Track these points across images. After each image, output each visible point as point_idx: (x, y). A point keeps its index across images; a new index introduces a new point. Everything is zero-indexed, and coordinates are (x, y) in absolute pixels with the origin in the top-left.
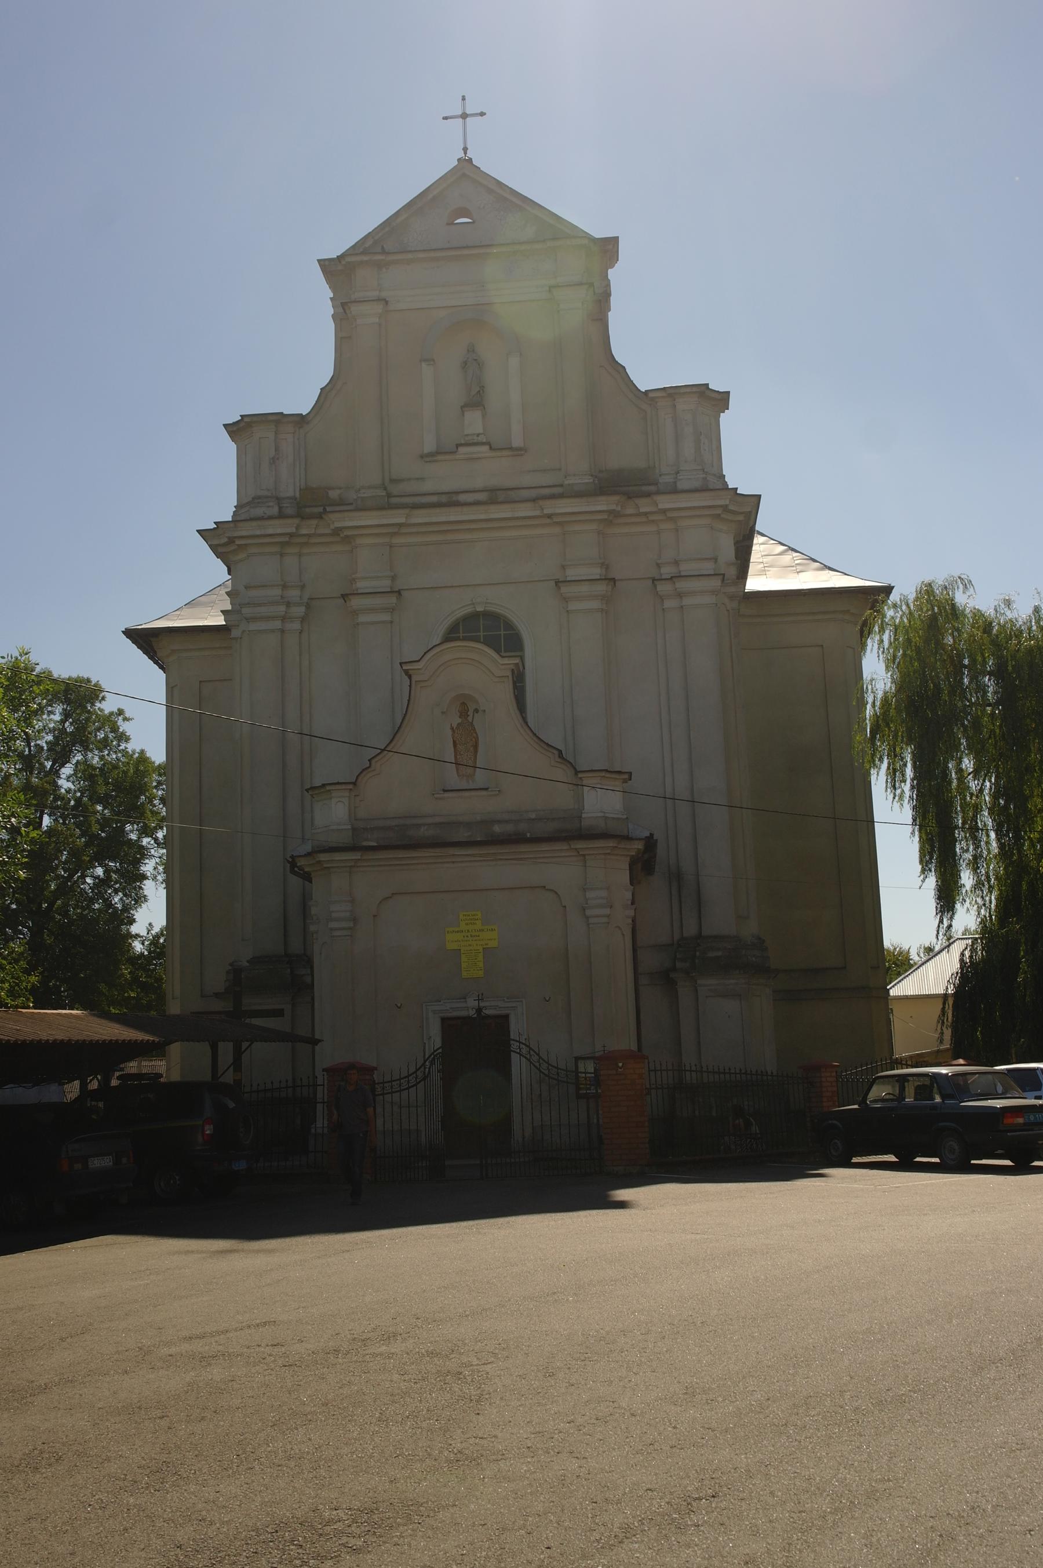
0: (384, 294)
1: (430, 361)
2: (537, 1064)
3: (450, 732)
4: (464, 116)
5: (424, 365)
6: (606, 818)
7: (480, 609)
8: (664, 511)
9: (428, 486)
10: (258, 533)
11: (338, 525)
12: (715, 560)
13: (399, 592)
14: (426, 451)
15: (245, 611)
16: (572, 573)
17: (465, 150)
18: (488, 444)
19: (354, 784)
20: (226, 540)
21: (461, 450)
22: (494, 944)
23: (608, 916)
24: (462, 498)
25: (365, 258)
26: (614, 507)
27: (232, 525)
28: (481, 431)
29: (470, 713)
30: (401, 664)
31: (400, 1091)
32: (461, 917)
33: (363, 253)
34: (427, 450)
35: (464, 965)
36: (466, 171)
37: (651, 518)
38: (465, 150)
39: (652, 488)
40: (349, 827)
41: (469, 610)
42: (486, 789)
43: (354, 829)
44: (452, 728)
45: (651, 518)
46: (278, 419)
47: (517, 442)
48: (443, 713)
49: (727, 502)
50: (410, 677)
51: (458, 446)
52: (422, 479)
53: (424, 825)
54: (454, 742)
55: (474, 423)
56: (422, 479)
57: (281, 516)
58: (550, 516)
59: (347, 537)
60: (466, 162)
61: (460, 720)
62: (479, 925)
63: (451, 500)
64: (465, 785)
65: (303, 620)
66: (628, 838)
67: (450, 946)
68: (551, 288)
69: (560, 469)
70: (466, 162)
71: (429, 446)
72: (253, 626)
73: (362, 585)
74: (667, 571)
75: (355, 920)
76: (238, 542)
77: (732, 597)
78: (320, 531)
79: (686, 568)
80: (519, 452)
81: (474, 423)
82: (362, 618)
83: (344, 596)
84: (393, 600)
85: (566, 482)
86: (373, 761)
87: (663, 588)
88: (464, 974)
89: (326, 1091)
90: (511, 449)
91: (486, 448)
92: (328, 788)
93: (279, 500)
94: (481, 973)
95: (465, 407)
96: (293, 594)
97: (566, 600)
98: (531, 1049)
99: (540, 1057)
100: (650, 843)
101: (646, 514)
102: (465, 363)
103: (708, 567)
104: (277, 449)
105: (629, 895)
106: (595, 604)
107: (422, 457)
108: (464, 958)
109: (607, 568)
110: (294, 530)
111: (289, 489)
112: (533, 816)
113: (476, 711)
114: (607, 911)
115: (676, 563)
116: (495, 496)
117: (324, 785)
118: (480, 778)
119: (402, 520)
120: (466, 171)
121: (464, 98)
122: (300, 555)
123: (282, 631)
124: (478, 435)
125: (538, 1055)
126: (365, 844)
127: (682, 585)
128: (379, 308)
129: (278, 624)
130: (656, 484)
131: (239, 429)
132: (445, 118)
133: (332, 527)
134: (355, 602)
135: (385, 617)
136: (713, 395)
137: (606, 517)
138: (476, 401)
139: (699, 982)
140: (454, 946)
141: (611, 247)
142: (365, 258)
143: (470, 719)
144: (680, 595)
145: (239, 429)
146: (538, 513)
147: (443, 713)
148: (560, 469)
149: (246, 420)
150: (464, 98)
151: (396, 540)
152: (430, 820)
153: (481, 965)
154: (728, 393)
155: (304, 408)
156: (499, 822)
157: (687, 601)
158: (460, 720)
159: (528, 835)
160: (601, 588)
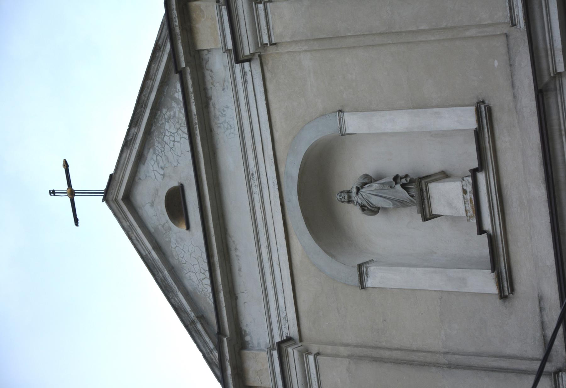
1: (362, 273)
4: (72, 193)
5: (369, 283)
14: (494, 289)
21: (487, 225)
47: (467, 119)
51: (481, 231)
52: (540, 299)
56: (540, 299)
68: (238, 57)
80: (485, 114)
81: (448, 197)
90: (478, 134)
91: (481, 177)
102: (363, 208)
107: (503, 296)
124: (465, 192)
128: (293, 353)
148: (507, 36)
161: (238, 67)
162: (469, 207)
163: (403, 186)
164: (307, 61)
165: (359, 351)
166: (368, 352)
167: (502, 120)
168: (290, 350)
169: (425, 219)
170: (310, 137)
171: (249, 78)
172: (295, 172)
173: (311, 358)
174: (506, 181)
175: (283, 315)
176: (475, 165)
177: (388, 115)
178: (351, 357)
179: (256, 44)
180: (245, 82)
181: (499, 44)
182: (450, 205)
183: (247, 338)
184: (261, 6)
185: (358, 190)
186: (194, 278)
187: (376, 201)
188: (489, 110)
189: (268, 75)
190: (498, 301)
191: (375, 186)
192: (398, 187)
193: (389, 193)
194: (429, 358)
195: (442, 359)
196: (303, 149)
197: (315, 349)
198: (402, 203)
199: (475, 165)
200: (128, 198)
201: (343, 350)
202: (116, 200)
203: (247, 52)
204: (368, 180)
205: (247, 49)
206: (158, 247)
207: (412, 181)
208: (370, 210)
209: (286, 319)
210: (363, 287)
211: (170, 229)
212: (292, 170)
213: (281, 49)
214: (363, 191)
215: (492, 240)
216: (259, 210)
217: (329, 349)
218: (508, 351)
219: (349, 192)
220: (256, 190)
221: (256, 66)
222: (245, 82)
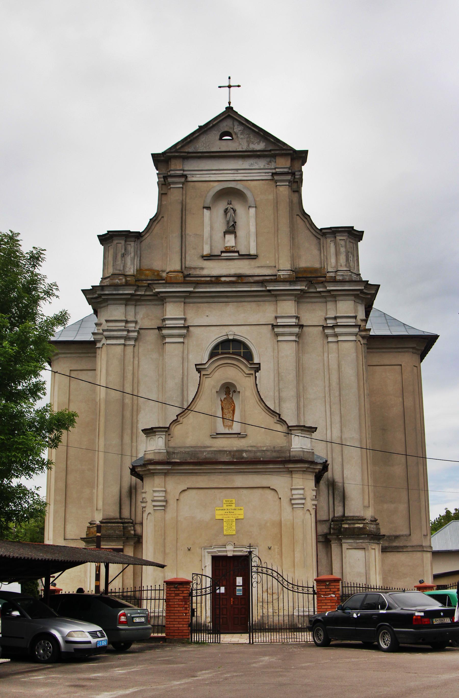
0: (185, 173)
1: (208, 208)
2: (282, 582)
3: (220, 403)
4: (230, 87)
5: (205, 210)
6: (304, 451)
7: (231, 337)
8: (330, 291)
9: (205, 272)
10: (114, 292)
11: (157, 290)
12: (355, 317)
13: (188, 327)
15: (105, 333)
16: (280, 321)
17: (230, 103)
18: (238, 252)
19: (168, 428)
20: (97, 295)
21: (223, 254)
22: (241, 517)
23: (303, 504)
24: (223, 279)
25: (177, 154)
26: (304, 288)
27: (100, 288)
28: (234, 245)
29: (231, 393)
30: (196, 365)
31: (201, 595)
32: (224, 502)
33: (176, 152)
34: (205, 253)
35: (225, 528)
36: (230, 113)
37: (323, 294)
38: (230, 103)
39: (323, 279)
40: (165, 451)
41: (225, 338)
42: (239, 434)
43: (168, 452)
44: (221, 400)
45: (323, 294)
46: (127, 235)
47: (253, 252)
48: (217, 392)
49: (363, 288)
50: (199, 372)
51: (222, 252)
52: (202, 268)
53: (205, 451)
54: (222, 409)
55: (230, 241)
57: (127, 284)
58: (269, 291)
59: (162, 297)
60: (229, 109)
61: (225, 396)
62: (233, 506)
63: (216, 280)
64: (228, 432)
65: (136, 339)
66: (313, 463)
67: (218, 517)
68: (273, 174)
69: (275, 267)
70: (229, 109)
71: (206, 251)
72: (109, 342)
73: (169, 323)
74: (330, 322)
75: (166, 501)
76: (103, 297)
77: (363, 337)
78: (148, 293)
79: (340, 321)
81: (230, 241)
82: (168, 340)
83: (160, 329)
84: (184, 331)
85: (279, 274)
86: (179, 417)
87: (328, 331)
88: (225, 533)
89: (165, 593)
90: (249, 255)
91: (237, 254)
92: (154, 430)
93: (126, 276)
94: (234, 533)
95: (225, 233)
96: (131, 326)
97: (277, 335)
98: (278, 574)
99: (283, 578)
100: (325, 466)
101: (320, 292)
102: (227, 209)
103: (351, 322)
104: (125, 249)
105: (314, 493)
106: (293, 338)
107: (203, 257)
108: (225, 524)
109: (299, 320)
110: (133, 292)
111: (131, 270)
112: (265, 449)
113: (234, 392)
114: (303, 501)
115: (335, 318)
116: (240, 278)
117: (152, 428)
118: (236, 428)
119: (191, 289)
120: (230, 113)
121: (229, 78)
122: (136, 306)
123: (124, 345)
124: (232, 247)
125: (282, 577)
126: (173, 460)
127: (337, 330)
128: (183, 180)
129: (122, 341)
130: (325, 277)
131: (106, 239)
132: (220, 87)
133: (154, 291)
134: (165, 332)
135: (181, 340)
136: (355, 233)
137: (299, 292)
138: (231, 229)
139: (343, 541)
140: (220, 517)
141: (304, 155)
142: (177, 154)
143: (231, 396)
144: (336, 335)
145: (106, 239)
146: (264, 289)
147: (217, 392)
149: (110, 233)
150: (229, 78)
151: (187, 300)
152: (209, 449)
153: (234, 528)
154: (363, 232)
155: (141, 228)
156: (246, 451)
157: (340, 338)
158: (225, 396)
159: (262, 459)
160: (296, 330)
161: (271, 174)
162: (228, 248)
163: (233, 225)
164: (271, 197)
165: (184, 203)
166: (184, 207)
167: (253, 262)
168: (184, 179)
169: (224, 232)
170: (249, 195)
171: (267, 174)
172: (238, 187)
173: (181, 186)
174: (236, 261)
175: (194, 176)
176: (240, 253)
177: (254, 224)
178: (182, 200)
179: (277, 180)
180: (266, 173)
181: (273, 264)
182: (228, 241)
183: (186, 160)
184: (288, 184)
185: (232, 208)
186: (204, 138)
187: (229, 214)
188: (255, 258)
189: (267, 181)
190: (201, 254)
191: (233, 215)
192: (233, 223)
193: (231, 219)
194: (184, 229)
195: (183, 233)
196: (245, 191)
197: (184, 187)
198: (228, 222)
199: (240, 253)
200: (229, 116)
201: (184, 197)
202: (229, 112)
203: (275, 177)
204: (235, 211)
205: (276, 178)
206: (214, 126)
207: (234, 227)
208: (226, 211)
209: (193, 177)
210: (204, 208)
211: (219, 132)
212: (239, 186)
213: (275, 187)
214: (232, 210)
215: (220, 256)
216: (227, 173)
217: (184, 192)
218: (187, 256)
219: (231, 204)
220: (233, 172)
221: (270, 178)
222: (266, 173)
